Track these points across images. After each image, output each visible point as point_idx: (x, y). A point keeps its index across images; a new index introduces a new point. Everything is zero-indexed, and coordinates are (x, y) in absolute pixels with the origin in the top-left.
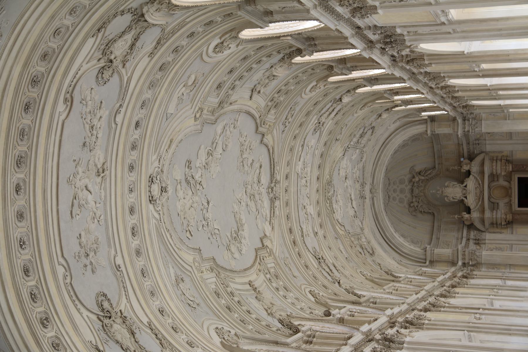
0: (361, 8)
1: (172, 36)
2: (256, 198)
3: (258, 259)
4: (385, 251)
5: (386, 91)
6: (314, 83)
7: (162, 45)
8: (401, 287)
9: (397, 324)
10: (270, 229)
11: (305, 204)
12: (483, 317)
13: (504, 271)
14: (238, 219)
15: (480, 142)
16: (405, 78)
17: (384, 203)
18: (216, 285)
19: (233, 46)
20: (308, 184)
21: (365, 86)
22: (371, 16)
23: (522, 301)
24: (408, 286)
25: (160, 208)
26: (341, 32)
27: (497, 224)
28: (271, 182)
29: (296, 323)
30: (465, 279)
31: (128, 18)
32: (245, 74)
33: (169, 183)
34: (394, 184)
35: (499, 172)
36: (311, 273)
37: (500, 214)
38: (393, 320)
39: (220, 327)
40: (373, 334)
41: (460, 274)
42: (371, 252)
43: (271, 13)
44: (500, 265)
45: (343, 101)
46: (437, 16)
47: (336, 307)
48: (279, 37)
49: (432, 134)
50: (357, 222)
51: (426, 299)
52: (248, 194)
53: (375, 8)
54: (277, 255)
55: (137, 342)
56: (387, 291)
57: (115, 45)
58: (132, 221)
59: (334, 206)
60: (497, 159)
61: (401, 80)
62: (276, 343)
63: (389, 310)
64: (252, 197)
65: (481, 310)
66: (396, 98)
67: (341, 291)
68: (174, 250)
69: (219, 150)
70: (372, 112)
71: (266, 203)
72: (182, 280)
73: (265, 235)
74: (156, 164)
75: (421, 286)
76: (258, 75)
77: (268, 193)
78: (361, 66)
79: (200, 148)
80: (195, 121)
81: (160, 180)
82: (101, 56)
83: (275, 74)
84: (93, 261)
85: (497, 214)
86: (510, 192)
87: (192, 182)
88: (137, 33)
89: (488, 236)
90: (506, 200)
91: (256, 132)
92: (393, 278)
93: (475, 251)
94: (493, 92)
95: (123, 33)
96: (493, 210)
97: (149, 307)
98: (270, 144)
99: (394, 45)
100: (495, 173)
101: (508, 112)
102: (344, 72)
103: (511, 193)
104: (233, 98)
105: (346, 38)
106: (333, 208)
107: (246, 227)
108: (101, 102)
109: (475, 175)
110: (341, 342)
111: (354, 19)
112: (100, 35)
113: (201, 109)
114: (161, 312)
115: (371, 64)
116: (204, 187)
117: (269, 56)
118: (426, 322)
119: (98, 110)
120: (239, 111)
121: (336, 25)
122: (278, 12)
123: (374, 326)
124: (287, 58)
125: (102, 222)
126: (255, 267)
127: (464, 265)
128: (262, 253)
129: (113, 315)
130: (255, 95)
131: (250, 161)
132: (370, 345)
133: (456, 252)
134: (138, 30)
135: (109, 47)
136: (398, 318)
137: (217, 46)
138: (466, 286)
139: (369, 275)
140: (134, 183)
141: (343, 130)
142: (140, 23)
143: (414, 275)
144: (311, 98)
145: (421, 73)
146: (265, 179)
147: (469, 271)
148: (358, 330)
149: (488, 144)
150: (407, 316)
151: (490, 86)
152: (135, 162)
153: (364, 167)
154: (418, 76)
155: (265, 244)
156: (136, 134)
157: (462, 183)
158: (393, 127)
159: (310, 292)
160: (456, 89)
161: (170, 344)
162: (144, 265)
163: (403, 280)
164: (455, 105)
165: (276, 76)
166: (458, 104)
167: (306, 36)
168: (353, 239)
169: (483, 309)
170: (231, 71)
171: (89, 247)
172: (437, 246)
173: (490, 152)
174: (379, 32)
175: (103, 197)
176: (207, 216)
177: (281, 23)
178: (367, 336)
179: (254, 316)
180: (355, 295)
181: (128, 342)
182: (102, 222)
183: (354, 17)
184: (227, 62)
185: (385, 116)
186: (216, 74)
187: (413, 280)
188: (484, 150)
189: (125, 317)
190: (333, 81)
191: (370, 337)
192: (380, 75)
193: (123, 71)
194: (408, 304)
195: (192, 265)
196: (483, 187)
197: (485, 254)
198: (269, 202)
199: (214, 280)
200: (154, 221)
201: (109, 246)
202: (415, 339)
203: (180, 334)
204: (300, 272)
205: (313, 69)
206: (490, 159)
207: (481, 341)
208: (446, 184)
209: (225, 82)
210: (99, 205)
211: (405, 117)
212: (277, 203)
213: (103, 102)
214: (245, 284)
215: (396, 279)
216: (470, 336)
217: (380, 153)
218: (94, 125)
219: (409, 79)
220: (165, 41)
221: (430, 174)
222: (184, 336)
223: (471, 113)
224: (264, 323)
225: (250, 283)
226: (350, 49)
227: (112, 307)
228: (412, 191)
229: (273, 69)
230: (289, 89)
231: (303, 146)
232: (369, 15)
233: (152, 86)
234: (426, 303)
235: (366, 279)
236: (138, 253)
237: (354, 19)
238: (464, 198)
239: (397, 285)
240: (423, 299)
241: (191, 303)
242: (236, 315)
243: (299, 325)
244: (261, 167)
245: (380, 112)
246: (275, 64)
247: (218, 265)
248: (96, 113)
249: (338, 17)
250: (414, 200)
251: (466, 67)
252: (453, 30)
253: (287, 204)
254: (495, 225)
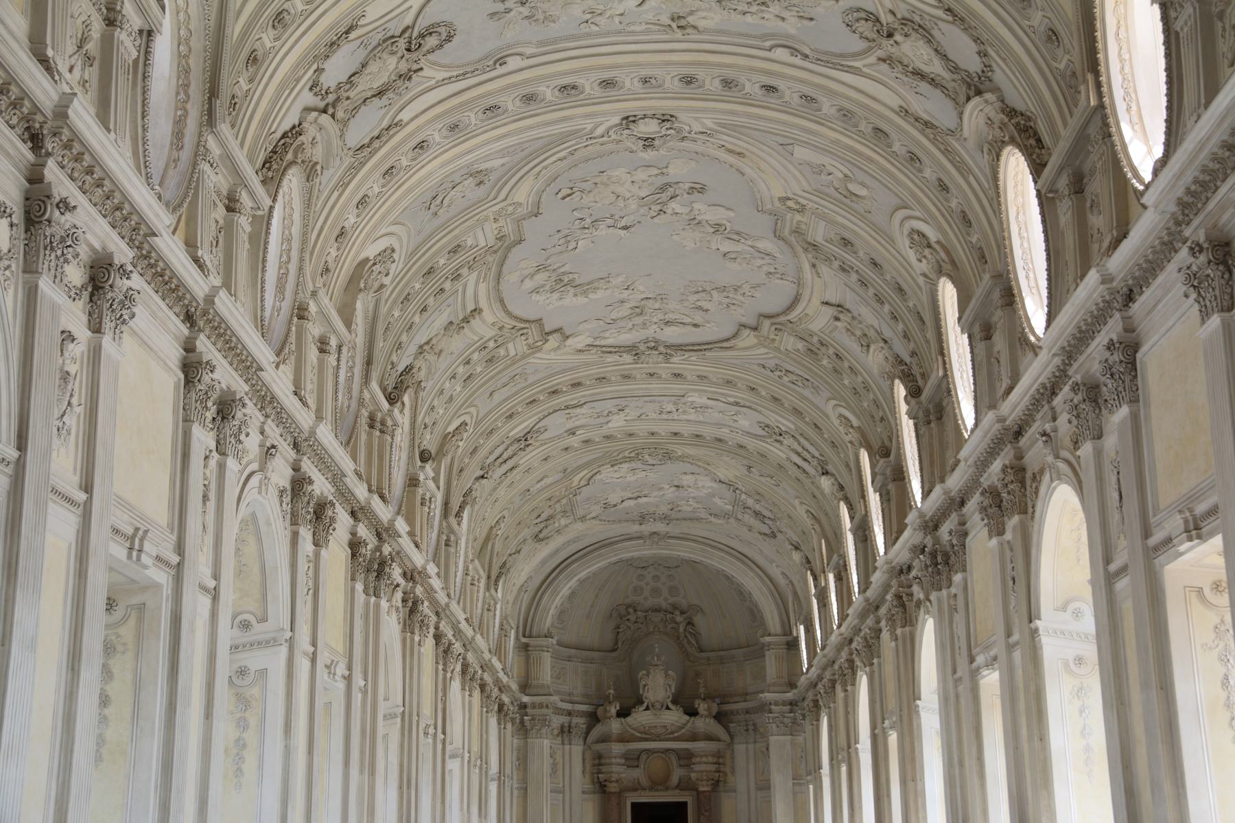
0: (1000, 507)
1: (940, 149)
2: (637, 318)
3: (523, 324)
4: (543, 562)
5: (843, 557)
6: (855, 423)
7: (922, 132)
8: (478, 591)
9: (411, 584)
10: (580, 346)
11: (627, 411)
12: (430, 740)
13: (515, 777)
14: (596, 284)
15: (751, 732)
16: (869, 593)
17: (632, 559)
18: (472, 248)
19: (924, 266)
20: (664, 416)
21: (852, 518)
22: (986, 525)
23: (462, 809)
24: (480, 605)
25: (614, 137)
26: (953, 470)
27: (600, 764)
28: (667, 347)
29: (406, 398)
30: (496, 708)
31: (973, 64)
32: (871, 291)
33: (662, 152)
34: (670, 576)
35: (696, 768)
36: (500, 425)
37: (618, 772)
38: (417, 578)
39: (396, 256)
40: (391, 540)
41: (506, 699)
42: (541, 536)
43: (988, 337)
44: (525, 770)
45: (823, 478)
46: (987, 648)
47: (438, 472)
48: (942, 354)
49: (763, 645)
50: (596, 510)
51: (458, 637)
52: (643, 302)
53: (1001, 532)
54: (532, 360)
55: (365, 101)
56: (471, 567)
57: (921, 43)
58: (589, 84)
59: (625, 466)
60: (719, 764)
61: (865, 585)
62: (369, 362)
63: (436, 570)
64: (638, 310)
65: (443, 736)
66: (831, 577)
67: (467, 481)
68: (535, 166)
69: (726, 246)
70: (804, 533)
71: (626, 338)
72: (481, 182)
73: (567, 337)
74: (697, 127)
75: (481, 628)
76: (868, 315)
77: (646, 341)
78: (890, 510)
79: (728, 209)
80: (779, 199)
81: (667, 135)
82: (899, 16)
83: (872, 347)
84: (512, 14)
85: (619, 764)
86: (659, 787)
87: (664, 196)
88: (944, 83)
89: (577, 749)
90: (645, 782)
91: (761, 315)
92: (494, 575)
93: (549, 726)
94: (845, 754)
95: (944, 57)
96: (627, 759)
97: (429, 122)
98: (739, 342)
99: (930, 569)
100: (693, 760)
101: (808, 782)
102: (879, 478)
103: (657, 790)
104: (824, 269)
105: (942, 481)
106: (621, 463)
107: (581, 300)
108: (811, 19)
109: (689, 725)
110: (374, 482)
111: (978, 494)
112: (940, 13)
113: (802, 210)
114: (421, 146)
115: (895, 528)
116: (656, 220)
117: (906, 336)
118: (417, 638)
119: (796, 14)
120: (799, 283)
121: (966, 460)
122: (989, 351)
123: (406, 543)
124: (903, 371)
125: (585, 29)
126: (507, 320)
127: (523, 706)
128: (534, 333)
129: (414, 56)
130: (830, 312)
131: (706, 305)
132: (371, 536)
133: (546, 692)
134: (950, 85)
135: (916, 31)
136: (423, 586)
137: (924, 236)
138: (485, 709)
139: (499, 532)
140: (659, 87)
141: (768, 479)
142: (964, 89)
143: (501, 616)
144: (828, 417)
145: (878, 622)
146: (672, 334)
147: (511, 715)
148: (398, 513)
149: (747, 748)
150: (426, 603)
151: (857, 749)
152: (700, 87)
153: (698, 519)
154: (872, 616)
156: (752, 88)
157: (674, 702)
158: (775, 572)
159: (464, 424)
160: (849, 688)
161: (363, 164)
162: (506, 111)
163: (491, 595)
164: (820, 686)
165: (868, 351)
166: (822, 691)
167: (944, 404)
168: (564, 501)
169: (444, 740)
170: (875, 264)
171: (538, 5)
172: (556, 657)
173: (733, 750)
174: (955, 542)
175: (632, 28)
176: (601, 227)
177: (969, 356)
178: (387, 530)
179: (417, 319)
180: (462, 508)
181: (366, 84)
182: (585, 29)
183: (982, 494)
184: (894, 256)
185: (796, 556)
186: (871, 236)
187: (491, 614)
188: (736, 741)
189: (410, 78)
190: (861, 458)
191: (384, 535)
192: (872, 546)
193: (872, 59)
194: (447, 605)
195: (509, 201)
196: (667, 740)
197: (544, 744)
198: (629, 343)
199: (483, 244)
200: (589, 127)
201: (541, 44)
202: (384, 617)
203: (382, 181)
204: (500, 404)
205: (882, 419)
206: (719, 752)
207: (386, 736)
208: (670, 672)
209: (855, 253)
210: (617, 22)
211: (795, 593)
212: (628, 358)
213: (813, 22)
214: (476, 302)
215: (493, 581)
216: (395, 716)
217: (727, 549)
218: (768, 7)
219: (867, 600)
220: (932, 136)
221: (689, 642)
222: (376, 190)
223: (804, 716)
224: (404, 338)
225: (477, 311)
226: (923, 487)
227: (429, 52)
228: (657, 610)
229: (882, 344)
230: (844, 375)
231: (737, 404)
232: (986, 521)
233: (845, 115)
234: (451, 638)
235: (492, 527)
236: (529, 98)
237: (978, 494)
238: (645, 704)
239: (482, 585)
240: (458, 632)
241: (438, 201)
242: (418, 286)
243: (403, 404)
244: (696, 325)
245: (803, 548)
246: (890, 348)
247: (509, 249)
248: (790, 10)
249: (983, 464)
250: (639, 613)
251: (892, 703)
252: (960, 679)
253: (627, 377)
254: (598, 762)
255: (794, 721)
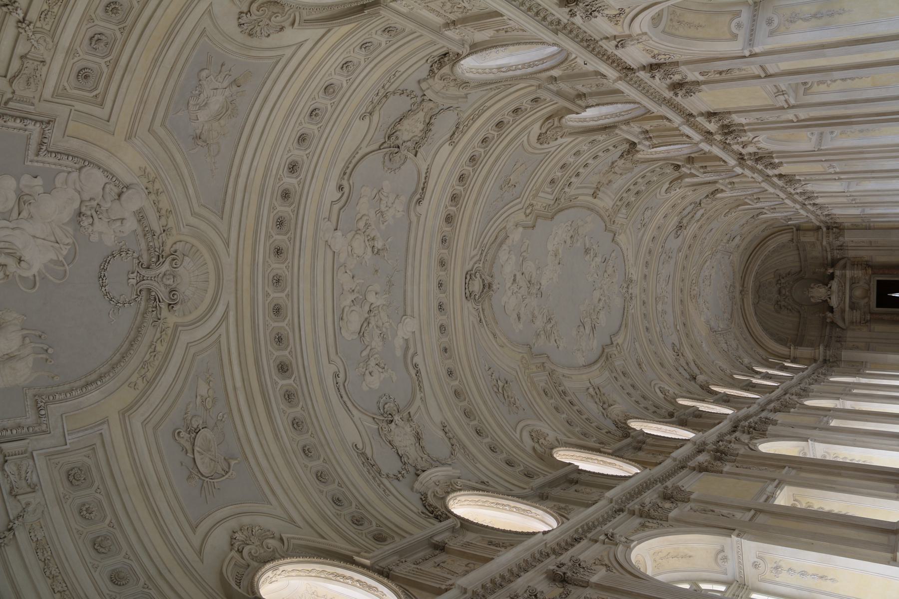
89: (849, 334)
90: (866, 300)
127: (825, 361)
155: (615, 343)
188: (847, 256)
254: (852, 323)
255: (836, 227)
